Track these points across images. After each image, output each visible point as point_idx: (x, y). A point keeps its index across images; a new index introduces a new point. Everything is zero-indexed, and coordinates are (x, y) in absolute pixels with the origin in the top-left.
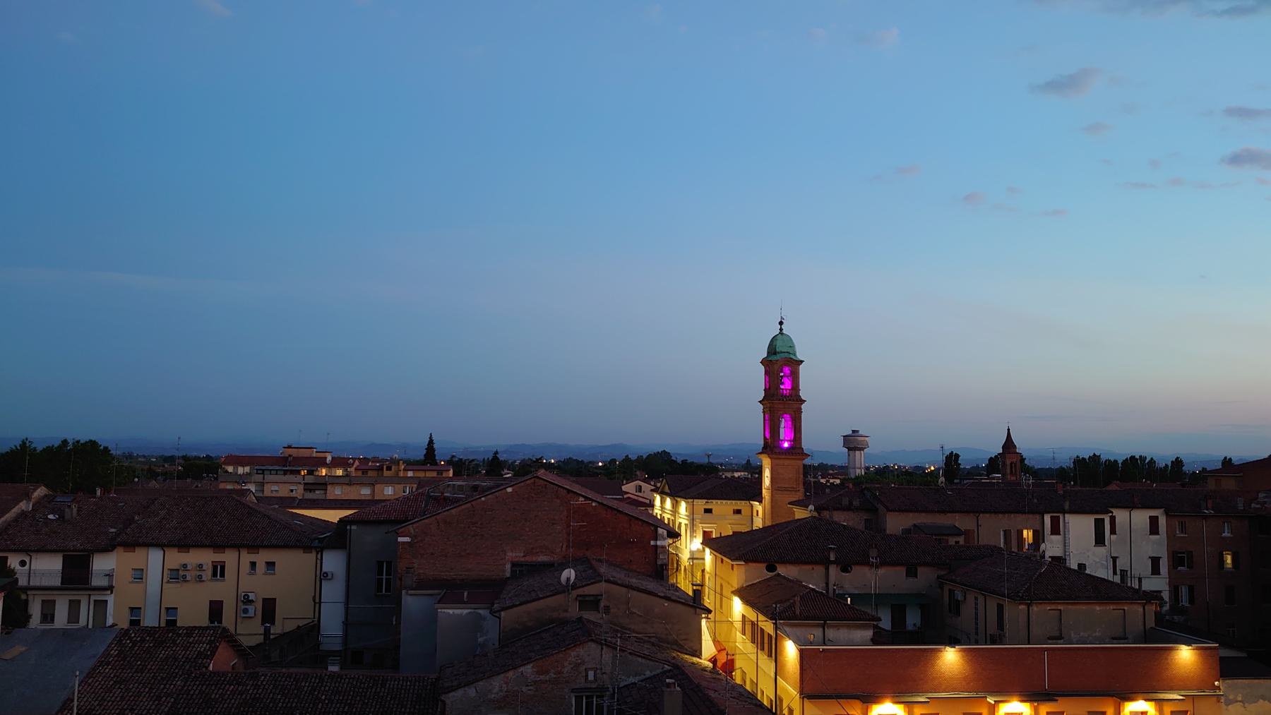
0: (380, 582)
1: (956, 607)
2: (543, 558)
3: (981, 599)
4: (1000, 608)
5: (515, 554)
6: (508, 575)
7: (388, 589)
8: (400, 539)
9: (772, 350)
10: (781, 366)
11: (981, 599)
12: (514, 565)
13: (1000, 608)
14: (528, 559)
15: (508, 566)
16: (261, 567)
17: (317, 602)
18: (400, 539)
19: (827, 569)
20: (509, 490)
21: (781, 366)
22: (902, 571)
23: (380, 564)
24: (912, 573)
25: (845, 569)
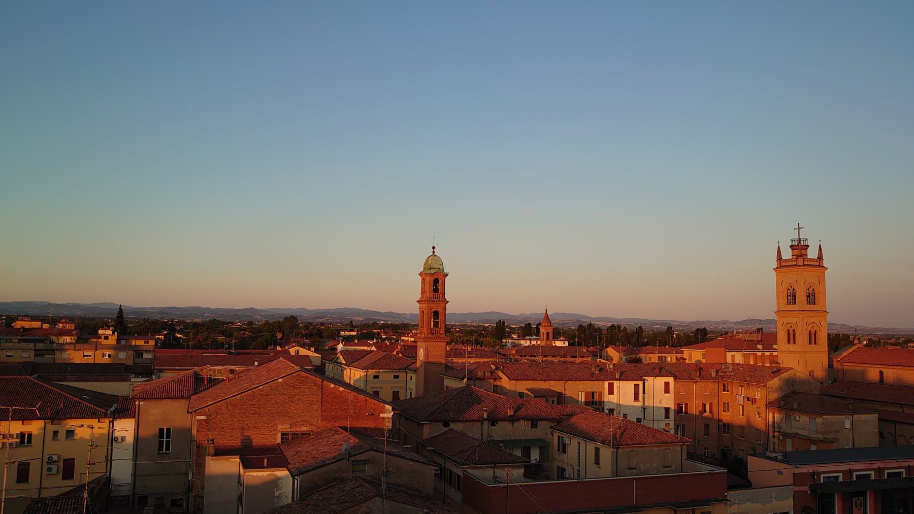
0: (161, 443)
1: (563, 448)
2: (304, 429)
3: (583, 444)
4: (597, 450)
5: (283, 427)
6: (279, 441)
7: (168, 449)
8: (198, 418)
9: (428, 266)
10: (434, 281)
11: (583, 444)
12: (283, 434)
13: (597, 450)
14: (294, 429)
15: (279, 436)
16: (62, 435)
17: (109, 460)
18: (198, 418)
19: (482, 423)
20: (280, 380)
21: (434, 281)
22: (530, 423)
23: (161, 430)
24: (534, 425)
25: (493, 424)
